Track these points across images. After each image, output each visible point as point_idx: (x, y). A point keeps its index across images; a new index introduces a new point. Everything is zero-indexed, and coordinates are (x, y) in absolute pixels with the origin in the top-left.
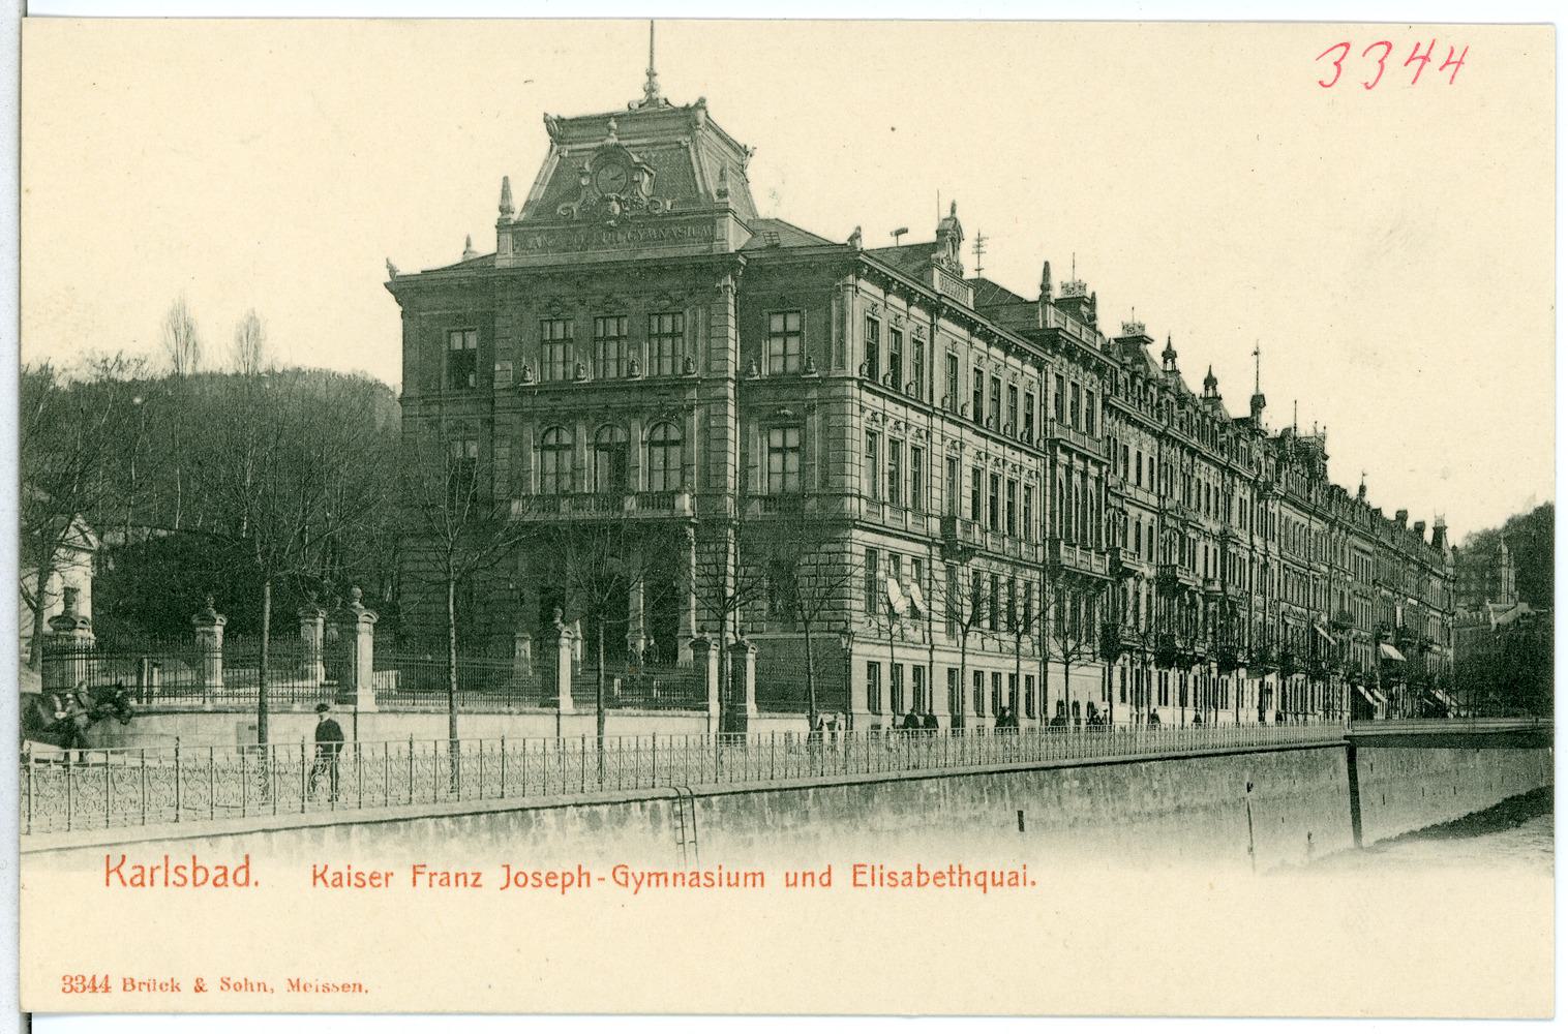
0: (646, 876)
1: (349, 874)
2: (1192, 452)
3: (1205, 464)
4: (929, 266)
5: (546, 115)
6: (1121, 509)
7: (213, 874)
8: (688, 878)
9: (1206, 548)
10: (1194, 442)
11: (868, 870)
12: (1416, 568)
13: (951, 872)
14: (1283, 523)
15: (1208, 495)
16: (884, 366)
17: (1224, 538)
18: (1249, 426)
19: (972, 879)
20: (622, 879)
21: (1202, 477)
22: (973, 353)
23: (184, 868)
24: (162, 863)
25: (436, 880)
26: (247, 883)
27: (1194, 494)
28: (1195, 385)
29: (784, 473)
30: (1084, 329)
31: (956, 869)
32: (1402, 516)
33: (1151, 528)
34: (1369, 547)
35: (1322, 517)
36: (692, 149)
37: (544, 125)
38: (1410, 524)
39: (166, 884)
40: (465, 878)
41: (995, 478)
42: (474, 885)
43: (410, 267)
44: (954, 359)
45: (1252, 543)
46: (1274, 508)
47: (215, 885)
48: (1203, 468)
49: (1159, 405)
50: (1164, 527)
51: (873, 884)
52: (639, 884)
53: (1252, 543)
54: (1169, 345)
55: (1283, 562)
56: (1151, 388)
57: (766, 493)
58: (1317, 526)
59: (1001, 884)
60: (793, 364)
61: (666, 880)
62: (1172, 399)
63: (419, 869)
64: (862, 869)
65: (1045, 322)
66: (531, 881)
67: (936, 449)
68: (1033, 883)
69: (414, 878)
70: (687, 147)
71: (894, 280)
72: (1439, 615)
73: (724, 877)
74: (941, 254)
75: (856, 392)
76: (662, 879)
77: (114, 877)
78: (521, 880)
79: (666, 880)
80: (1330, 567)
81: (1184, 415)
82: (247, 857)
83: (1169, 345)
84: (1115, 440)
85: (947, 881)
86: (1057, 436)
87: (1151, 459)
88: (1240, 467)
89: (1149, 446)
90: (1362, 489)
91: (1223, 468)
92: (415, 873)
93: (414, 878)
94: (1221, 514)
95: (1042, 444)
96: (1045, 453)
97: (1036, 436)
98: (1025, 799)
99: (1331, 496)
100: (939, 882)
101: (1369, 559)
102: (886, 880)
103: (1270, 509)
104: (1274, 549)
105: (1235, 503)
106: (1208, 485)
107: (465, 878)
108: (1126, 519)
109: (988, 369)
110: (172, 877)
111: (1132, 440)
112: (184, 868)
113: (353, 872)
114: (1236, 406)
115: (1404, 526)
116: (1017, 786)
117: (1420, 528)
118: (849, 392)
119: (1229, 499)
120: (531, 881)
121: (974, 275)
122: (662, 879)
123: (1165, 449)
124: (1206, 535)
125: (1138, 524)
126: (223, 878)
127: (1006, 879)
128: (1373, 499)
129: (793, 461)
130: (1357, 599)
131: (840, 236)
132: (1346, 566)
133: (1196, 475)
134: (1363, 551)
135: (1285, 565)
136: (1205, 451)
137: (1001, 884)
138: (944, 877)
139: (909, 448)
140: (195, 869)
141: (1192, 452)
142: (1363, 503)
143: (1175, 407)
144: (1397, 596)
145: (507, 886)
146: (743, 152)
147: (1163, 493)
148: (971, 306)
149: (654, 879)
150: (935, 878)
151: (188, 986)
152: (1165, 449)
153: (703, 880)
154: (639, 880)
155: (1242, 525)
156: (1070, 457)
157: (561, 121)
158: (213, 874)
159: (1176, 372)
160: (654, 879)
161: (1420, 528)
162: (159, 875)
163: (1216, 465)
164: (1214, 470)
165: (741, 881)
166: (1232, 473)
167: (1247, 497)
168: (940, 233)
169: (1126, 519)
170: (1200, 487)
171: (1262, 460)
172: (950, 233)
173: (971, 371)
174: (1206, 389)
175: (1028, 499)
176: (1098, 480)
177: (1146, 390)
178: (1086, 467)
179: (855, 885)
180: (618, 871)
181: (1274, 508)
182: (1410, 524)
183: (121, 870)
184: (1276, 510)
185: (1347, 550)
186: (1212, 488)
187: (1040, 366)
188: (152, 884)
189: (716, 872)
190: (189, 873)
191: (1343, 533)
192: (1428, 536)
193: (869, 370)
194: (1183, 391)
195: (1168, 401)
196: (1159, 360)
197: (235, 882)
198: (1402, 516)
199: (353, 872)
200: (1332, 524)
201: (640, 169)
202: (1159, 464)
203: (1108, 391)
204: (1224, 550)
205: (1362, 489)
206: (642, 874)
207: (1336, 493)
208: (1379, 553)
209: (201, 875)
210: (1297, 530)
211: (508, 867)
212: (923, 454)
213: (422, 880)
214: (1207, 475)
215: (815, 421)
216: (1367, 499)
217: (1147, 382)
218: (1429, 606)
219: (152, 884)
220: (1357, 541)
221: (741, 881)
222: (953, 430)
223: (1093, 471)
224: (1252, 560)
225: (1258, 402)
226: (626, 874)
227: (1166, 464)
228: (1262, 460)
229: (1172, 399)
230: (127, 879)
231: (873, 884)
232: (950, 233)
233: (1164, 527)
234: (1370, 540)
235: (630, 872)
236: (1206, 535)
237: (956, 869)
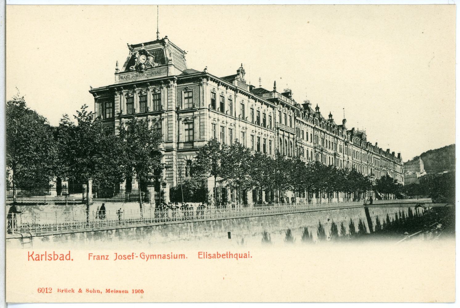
0: (150, 256)
1: (207, 255)
2: (324, 133)
3: (328, 136)
4: (234, 80)
5: (128, 44)
6: (301, 147)
7: (59, 256)
8: (162, 256)
9: (330, 157)
10: (325, 130)
11: (203, 254)
12: (393, 163)
13: (227, 254)
14: (353, 151)
15: (330, 144)
16: (261, 122)
17: (335, 155)
18: (342, 127)
19: (233, 256)
20: (143, 257)
21: (327, 139)
22: (249, 103)
23: (51, 255)
24: (45, 254)
25: (96, 258)
26: (69, 259)
27: (325, 143)
28: (327, 118)
29: (189, 136)
30: (288, 99)
31: (228, 253)
32: (388, 150)
33: (312, 152)
34: (379, 158)
35: (365, 150)
36: (164, 50)
37: (128, 47)
38: (391, 152)
39: (46, 260)
40: (104, 257)
41: (259, 138)
42: (106, 259)
43: (96, 86)
44: (243, 105)
45: (344, 156)
46: (350, 147)
47: (60, 260)
48: (328, 137)
49: (313, 120)
50: (316, 151)
51: (204, 258)
52: (148, 259)
53: (344, 156)
54: (317, 106)
55: (353, 161)
56: (310, 116)
57: (184, 141)
58: (364, 152)
59: (242, 257)
60: (191, 106)
61: (156, 257)
62: (317, 119)
63: (90, 255)
64: (201, 253)
65: (275, 97)
66: (123, 257)
67: (208, 120)
68: (251, 257)
69: (89, 257)
70: (163, 50)
71: (228, 86)
72: (400, 174)
73: (173, 256)
74: (238, 77)
75: (208, 112)
76: (155, 257)
77: (30, 258)
78: (120, 257)
79: (156, 257)
80: (368, 162)
81: (321, 123)
82: (70, 252)
83: (317, 106)
84: (299, 129)
85: (226, 256)
86: (279, 127)
87: (311, 134)
88: (340, 137)
89: (310, 131)
90: (376, 143)
91: (334, 137)
92: (89, 256)
93: (89, 257)
94: (334, 149)
95: (274, 129)
96: (275, 131)
97: (273, 126)
98: (231, 228)
99: (367, 145)
100: (224, 257)
101: (379, 161)
102: (208, 256)
103: (349, 148)
104: (350, 157)
105: (338, 146)
106: (329, 141)
107: (104, 257)
108: (303, 149)
109: (262, 111)
110: (48, 258)
111: (304, 129)
112: (51, 255)
113: (208, 254)
114: (338, 122)
115: (389, 153)
116: (228, 224)
117: (393, 153)
118: (205, 112)
119: (336, 144)
120: (123, 257)
121: (259, 87)
122: (155, 257)
123: (315, 132)
124: (329, 154)
125: (307, 151)
126: (62, 258)
127: (243, 256)
128: (379, 146)
129: (191, 132)
130: (376, 170)
131: (202, 70)
132: (372, 162)
133: (326, 139)
134: (377, 159)
135: (354, 162)
136: (328, 132)
137: (242, 257)
138: (130, 256)
139: (219, 126)
140: (54, 255)
141: (324, 133)
142: (377, 147)
143: (318, 121)
144: (387, 169)
145: (116, 259)
146: (183, 52)
147: (315, 143)
148: (249, 91)
149: (152, 257)
150: (222, 255)
151: (76, 290)
152: (315, 132)
153: (166, 257)
154: (148, 257)
155: (340, 151)
156: (284, 132)
157: (132, 46)
158: (59, 256)
159: (319, 113)
160: (152, 257)
161: (393, 153)
162: (44, 257)
163: (333, 136)
164: (331, 137)
165: (178, 256)
166: (337, 138)
167: (342, 144)
168: (238, 71)
169: (303, 149)
170: (327, 142)
171: (346, 135)
172: (241, 71)
173: (249, 108)
174: (316, 110)
175: (270, 144)
176: (294, 139)
177: (309, 117)
178: (289, 135)
179: (199, 258)
180: (142, 255)
181: (350, 147)
182: (391, 152)
183: (33, 256)
184: (351, 148)
185: (372, 158)
186: (331, 142)
187: (273, 108)
188: (42, 260)
189: (171, 254)
190: (52, 256)
191: (371, 154)
192: (396, 155)
193: (258, 123)
194: (321, 117)
195: (316, 119)
196: (315, 110)
197: (66, 259)
198: (388, 150)
199: (208, 254)
200: (368, 152)
201: (150, 56)
202: (314, 136)
203: (296, 116)
204: (335, 157)
205: (376, 143)
206: (149, 255)
207: (369, 144)
208: (382, 159)
209: (56, 257)
210: (357, 153)
211: (116, 254)
212: (233, 131)
213: (92, 258)
214: (330, 139)
215: (196, 121)
216: (378, 146)
217: (309, 114)
218: (397, 172)
219: (42, 260)
220: (375, 156)
221: (178, 256)
222: (243, 124)
223: (291, 136)
224: (344, 160)
225: (344, 121)
226: (144, 255)
227: (297, 128)
228: (346, 135)
229: (317, 119)
230: (34, 258)
231: (204, 258)
232: (241, 71)
233: (316, 151)
234: (379, 156)
235: (145, 254)
236: (329, 154)
237: (228, 253)
